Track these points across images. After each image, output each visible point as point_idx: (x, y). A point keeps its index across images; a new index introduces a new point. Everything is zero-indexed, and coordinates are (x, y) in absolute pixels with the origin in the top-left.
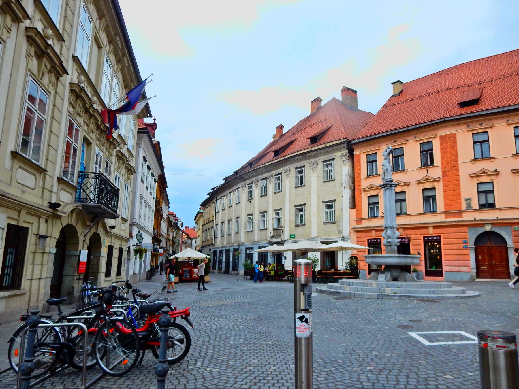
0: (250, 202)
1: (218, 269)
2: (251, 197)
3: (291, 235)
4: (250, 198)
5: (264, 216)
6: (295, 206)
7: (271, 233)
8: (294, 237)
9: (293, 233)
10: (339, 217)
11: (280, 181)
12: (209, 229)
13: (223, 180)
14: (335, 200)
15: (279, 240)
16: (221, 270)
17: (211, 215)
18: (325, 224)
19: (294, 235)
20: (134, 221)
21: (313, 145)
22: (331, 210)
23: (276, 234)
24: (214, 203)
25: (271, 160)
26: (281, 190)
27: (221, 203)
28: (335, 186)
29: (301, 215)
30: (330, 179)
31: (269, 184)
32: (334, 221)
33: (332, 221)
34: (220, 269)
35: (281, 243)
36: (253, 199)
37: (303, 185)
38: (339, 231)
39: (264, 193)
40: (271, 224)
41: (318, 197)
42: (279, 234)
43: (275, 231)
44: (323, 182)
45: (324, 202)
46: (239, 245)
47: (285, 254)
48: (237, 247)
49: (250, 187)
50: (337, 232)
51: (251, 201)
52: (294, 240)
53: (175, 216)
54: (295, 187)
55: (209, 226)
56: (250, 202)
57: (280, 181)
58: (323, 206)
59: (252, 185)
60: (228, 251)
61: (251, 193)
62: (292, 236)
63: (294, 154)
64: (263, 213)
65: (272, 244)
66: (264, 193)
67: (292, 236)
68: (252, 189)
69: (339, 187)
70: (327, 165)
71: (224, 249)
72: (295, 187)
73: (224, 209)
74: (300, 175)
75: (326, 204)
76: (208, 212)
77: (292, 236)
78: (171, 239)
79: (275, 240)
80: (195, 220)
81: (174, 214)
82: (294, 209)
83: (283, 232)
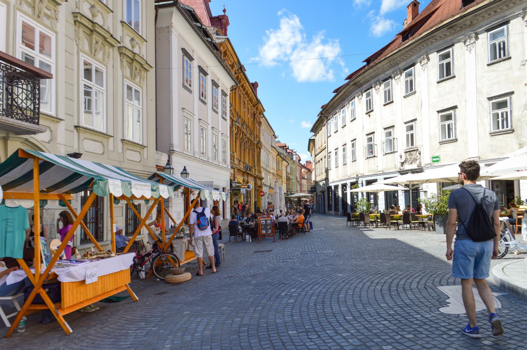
0: (369, 116)
1: (335, 210)
2: (370, 109)
3: (433, 158)
4: (369, 111)
5: (390, 134)
6: (439, 112)
7: (401, 157)
8: (438, 161)
9: (436, 154)
10: (519, 120)
11: (413, 77)
12: (321, 159)
13: (334, 92)
14: (512, 93)
15: (414, 166)
16: (338, 211)
17: (323, 142)
18: (492, 134)
19: (438, 157)
20: (171, 148)
21: (466, 7)
22: (504, 110)
23: (408, 157)
24: (325, 125)
25: (397, 47)
26: (414, 91)
27: (334, 123)
28: (511, 68)
29: (449, 125)
30: (500, 57)
31: (396, 84)
32: (509, 128)
33: (505, 129)
34: (337, 209)
35: (419, 170)
36: (372, 111)
37: (452, 75)
38: (520, 144)
39: (389, 101)
40: (401, 145)
41: (478, 91)
42: (413, 157)
43: (408, 153)
44: (488, 65)
45: (490, 99)
46: (358, 177)
47: (424, 187)
48: (354, 180)
49: (368, 95)
50: (517, 146)
51: (371, 114)
52: (439, 164)
53: (288, 148)
54: (438, 83)
55: (322, 156)
56: (369, 116)
57: (413, 77)
58: (488, 105)
59: (370, 90)
60: (344, 186)
61: (369, 104)
62: (435, 159)
63: (434, 29)
64: (389, 129)
65: (403, 173)
66: (389, 101)
67: (435, 159)
68: (370, 97)
69: (520, 69)
70: (494, 37)
71: (340, 184)
72: (438, 83)
73: (337, 131)
74: (445, 62)
75: (494, 101)
76: (320, 138)
77: (436, 159)
78: (284, 175)
79: (407, 167)
80: (309, 150)
81: (286, 146)
82: (437, 117)
83: (420, 154)
